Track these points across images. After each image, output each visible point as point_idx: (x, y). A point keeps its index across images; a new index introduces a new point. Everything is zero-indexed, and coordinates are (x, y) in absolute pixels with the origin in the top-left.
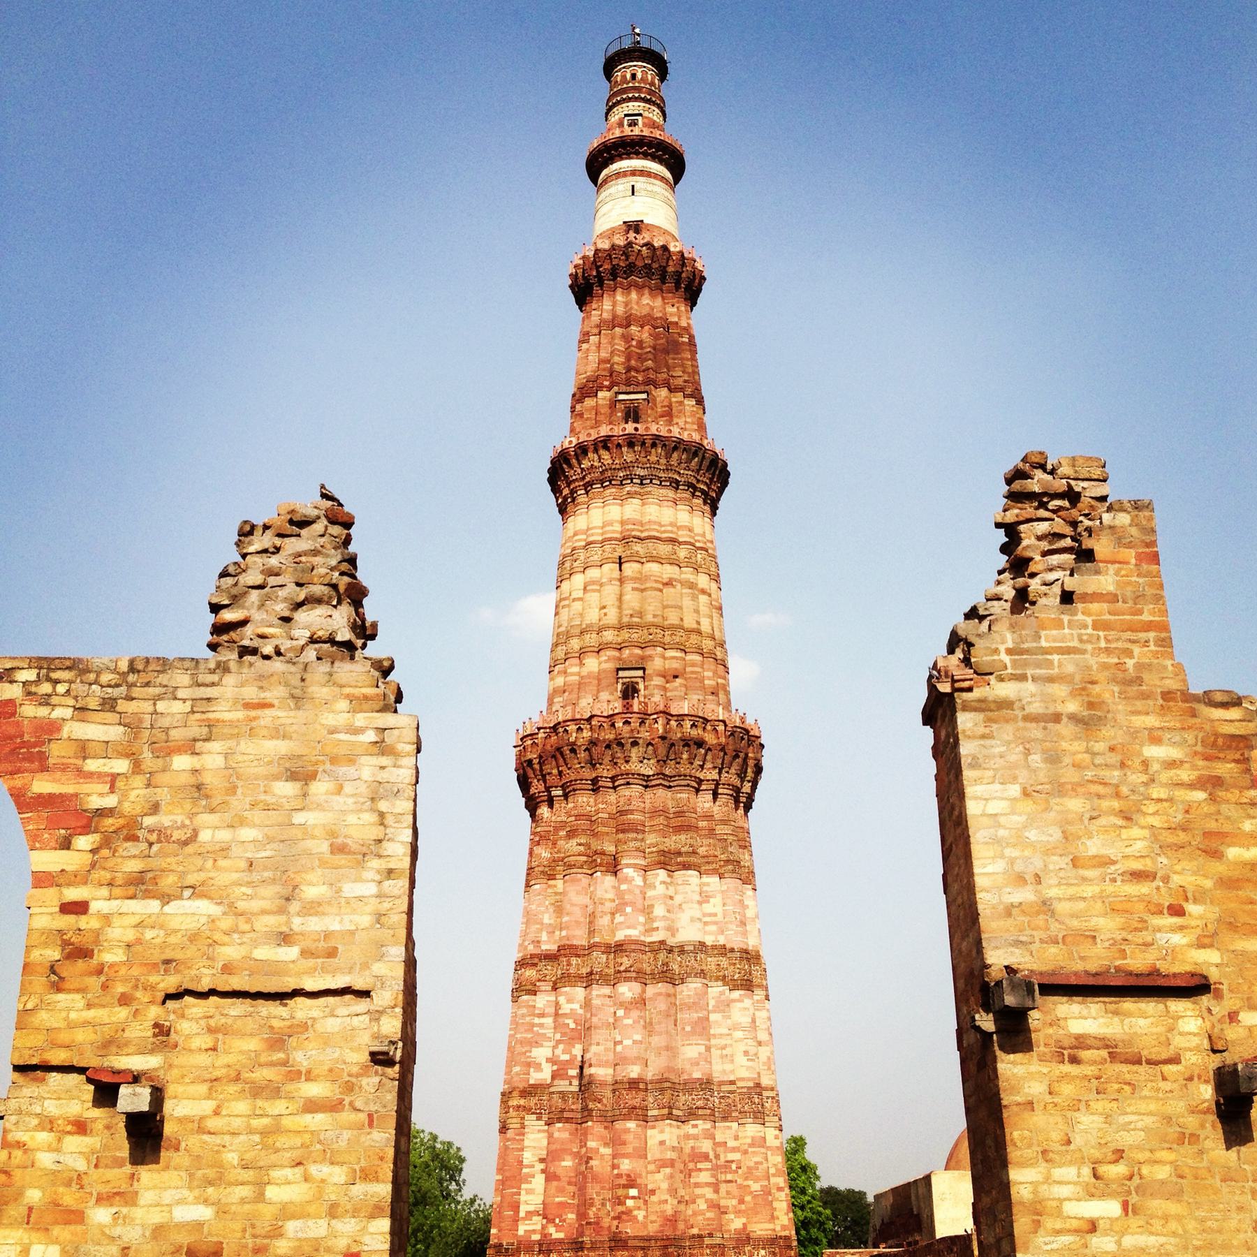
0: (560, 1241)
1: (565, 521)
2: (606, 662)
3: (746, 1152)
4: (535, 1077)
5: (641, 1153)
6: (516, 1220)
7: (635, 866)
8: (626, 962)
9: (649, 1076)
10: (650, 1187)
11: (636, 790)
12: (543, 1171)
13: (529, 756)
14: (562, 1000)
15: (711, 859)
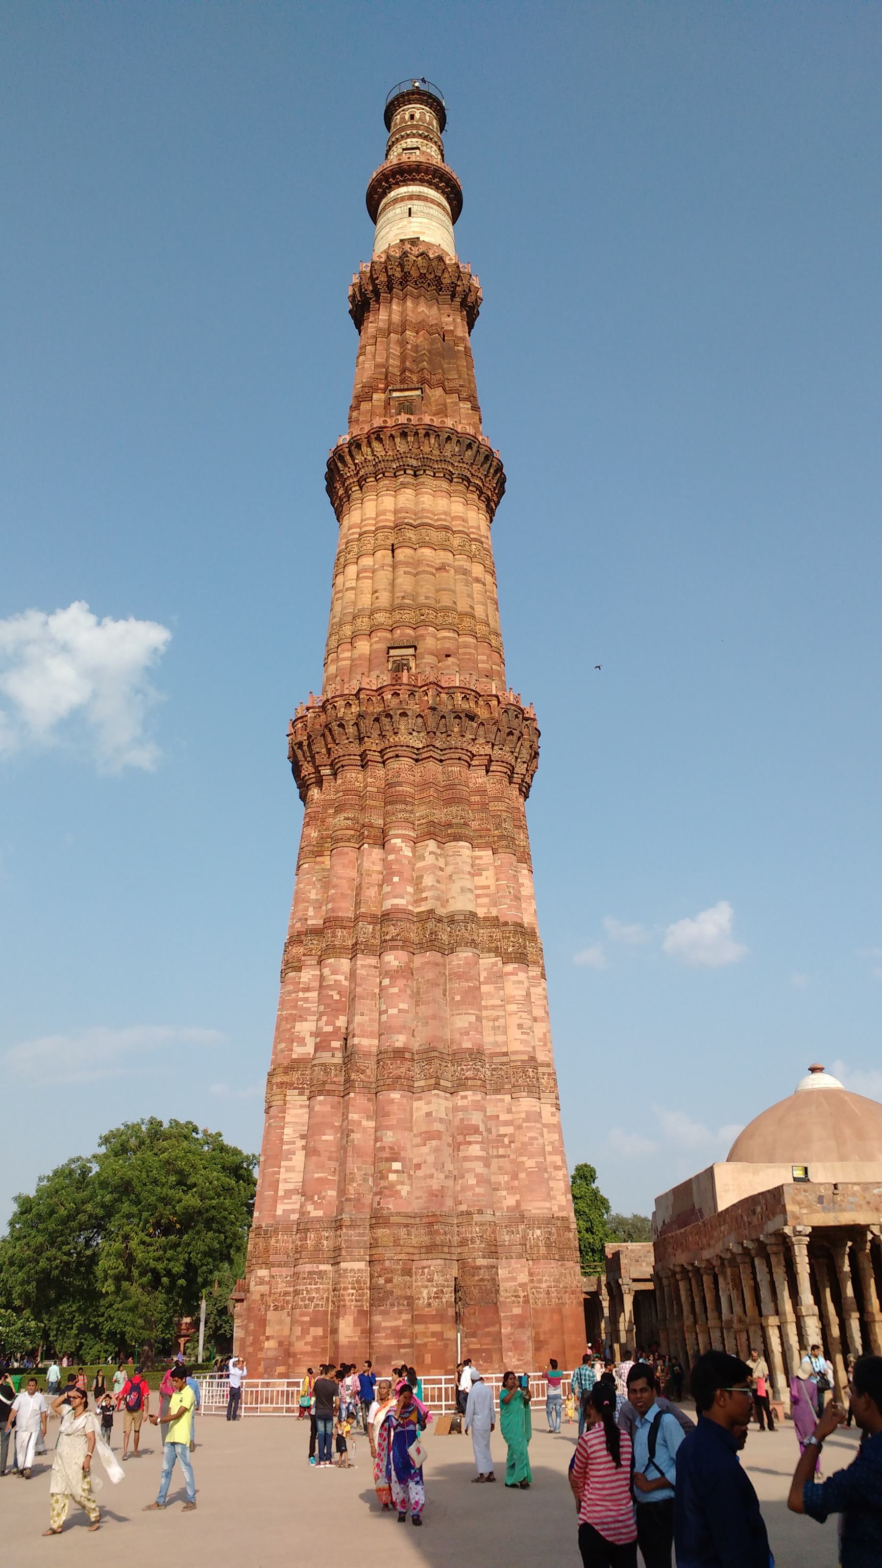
0: (318, 1220)
1: (339, 514)
2: (376, 642)
3: (520, 1127)
4: (298, 1051)
5: (407, 1125)
6: (275, 1200)
7: (403, 837)
8: (392, 931)
9: (416, 1046)
10: (415, 1161)
11: (405, 762)
12: (304, 1148)
13: (300, 738)
14: (326, 971)
15: (483, 833)
